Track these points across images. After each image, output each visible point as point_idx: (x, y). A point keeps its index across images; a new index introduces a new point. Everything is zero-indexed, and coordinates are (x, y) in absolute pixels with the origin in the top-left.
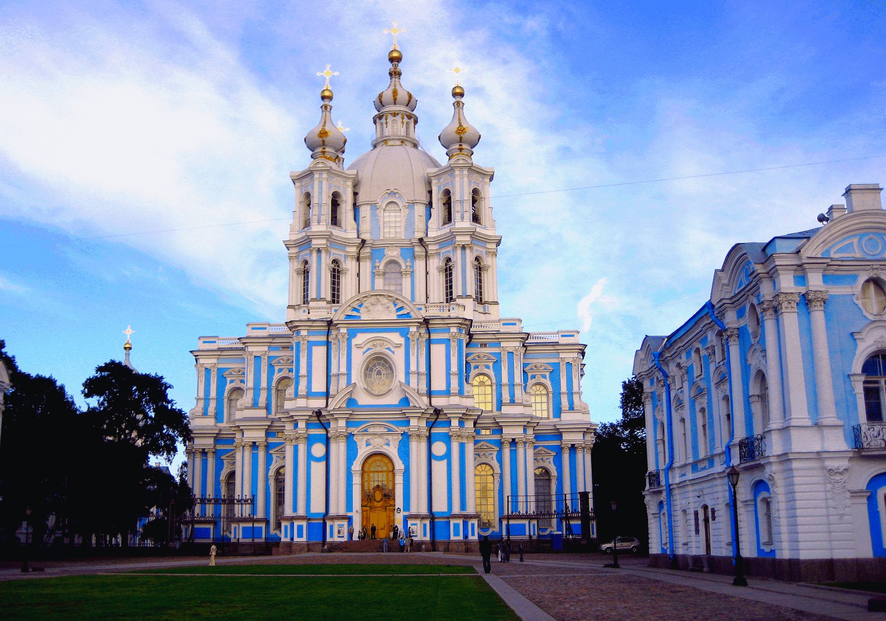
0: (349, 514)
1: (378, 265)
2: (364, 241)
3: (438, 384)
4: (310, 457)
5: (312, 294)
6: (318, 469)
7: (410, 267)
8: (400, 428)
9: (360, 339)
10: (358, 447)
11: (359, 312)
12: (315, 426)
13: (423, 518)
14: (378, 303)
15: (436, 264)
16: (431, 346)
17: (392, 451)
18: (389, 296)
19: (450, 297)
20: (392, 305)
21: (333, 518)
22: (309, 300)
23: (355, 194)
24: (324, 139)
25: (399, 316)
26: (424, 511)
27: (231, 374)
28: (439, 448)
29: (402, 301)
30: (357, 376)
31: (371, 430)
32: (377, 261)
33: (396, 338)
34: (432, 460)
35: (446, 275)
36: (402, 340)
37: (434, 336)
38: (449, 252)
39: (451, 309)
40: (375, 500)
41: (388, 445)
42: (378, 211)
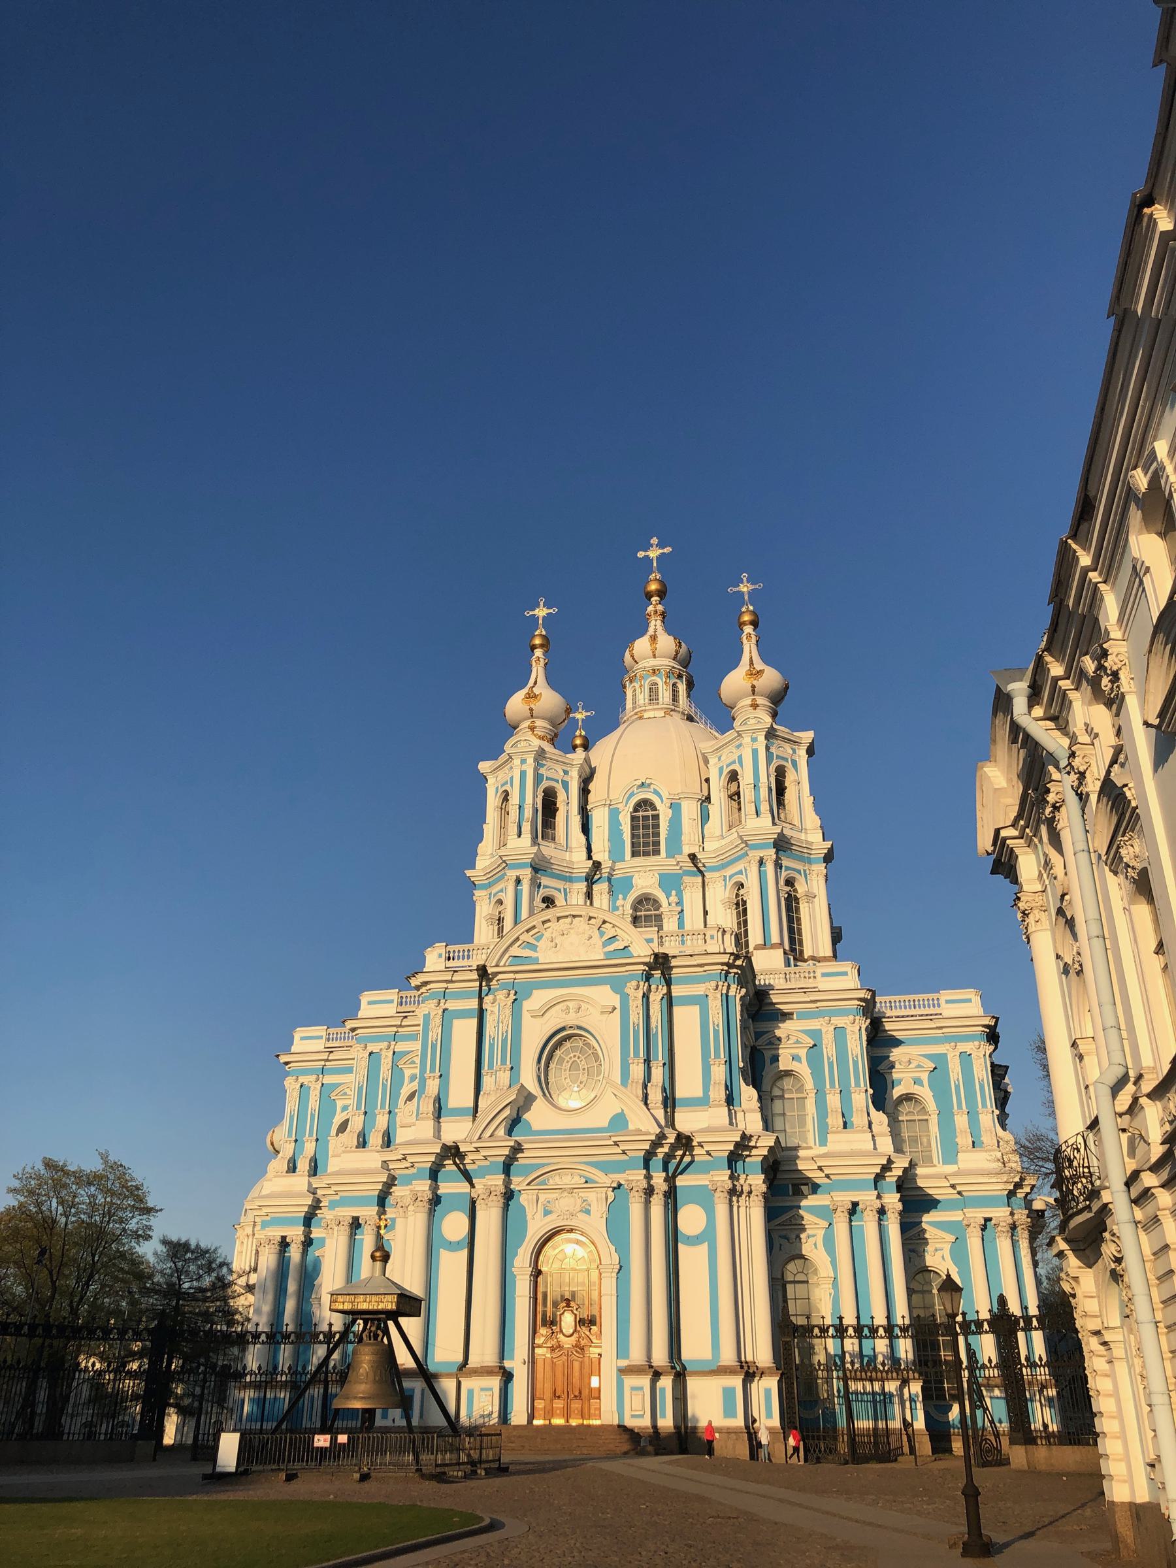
0: (507, 1364)
2: (597, 865)
3: (688, 1085)
7: (677, 904)
8: (611, 1176)
9: (539, 998)
10: (529, 1217)
11: (536, 951)
14: (572, 931)
15: (719, 893)
16: (676, 1010)
18: (590, 918)
20: (596, 934)
24: (532, 706)
25: (605, 954)
26: (660, 1356)
27: (345, 1094)
28: (691, 1219)
29: (614, 926)
31: (555, 1180)
32: (621, 896)
33: (605, 996)
34: (679, 1244)
35: (738, 913)
36: (616, 1000)
37: (676, 991)
38: (740, 872)
39: (708, 938)
40: (561, 1331)
41: (588, 1212)
42: (620, 817)
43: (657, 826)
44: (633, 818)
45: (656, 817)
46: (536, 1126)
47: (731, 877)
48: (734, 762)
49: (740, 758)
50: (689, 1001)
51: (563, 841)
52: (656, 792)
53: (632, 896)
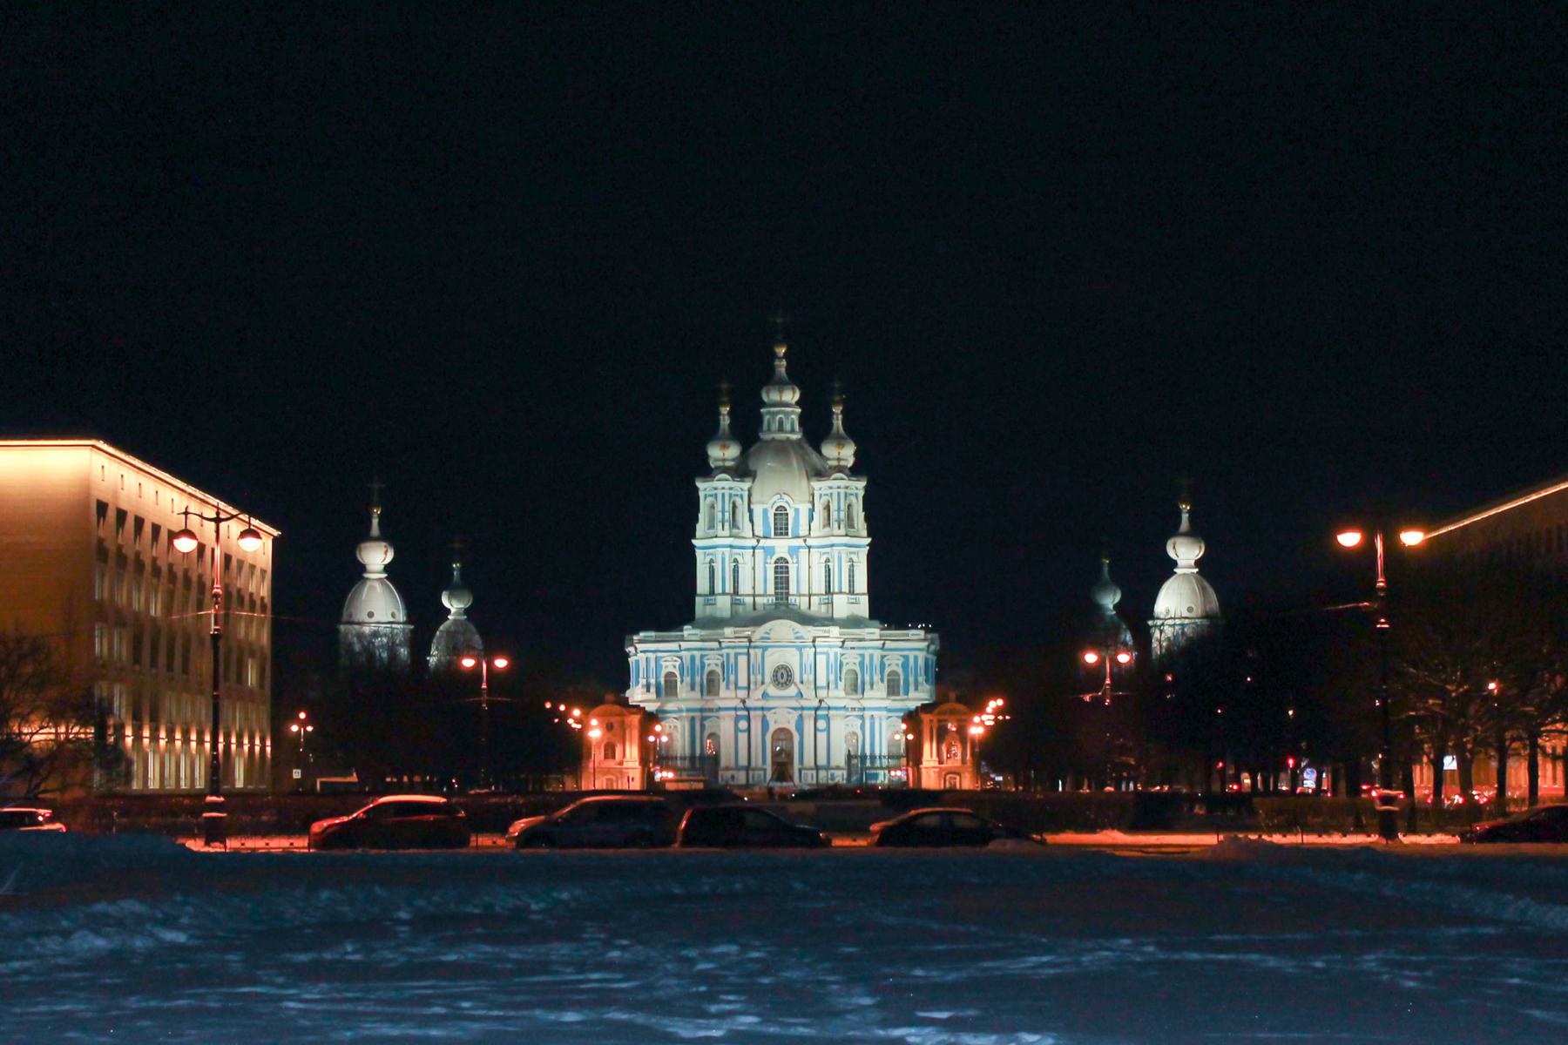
0: (765, 767)
1: (768, 561)
3: (821, 682)
4: (737, 730)
5: (718, 589)
6: (743, 737)
12: (742, 709)
13: (811, 769)
15: (818, 559)
17: (792, 727)
19: (828, 592)
21: (754, 770)
22: (716, 592)
23: (750, 496)
26: (812, 764)
28: (822, 724)
30: (768, 678)
43: (787, 519)
44: (775, 514)
45: (787, 514)
46: (771, 694)
47: (824, 553)
48: (827, 495)
49: (831, 494)
50: (821, 653)
51: (741, 527)
52: (787, 502)
53: (774, 558)
